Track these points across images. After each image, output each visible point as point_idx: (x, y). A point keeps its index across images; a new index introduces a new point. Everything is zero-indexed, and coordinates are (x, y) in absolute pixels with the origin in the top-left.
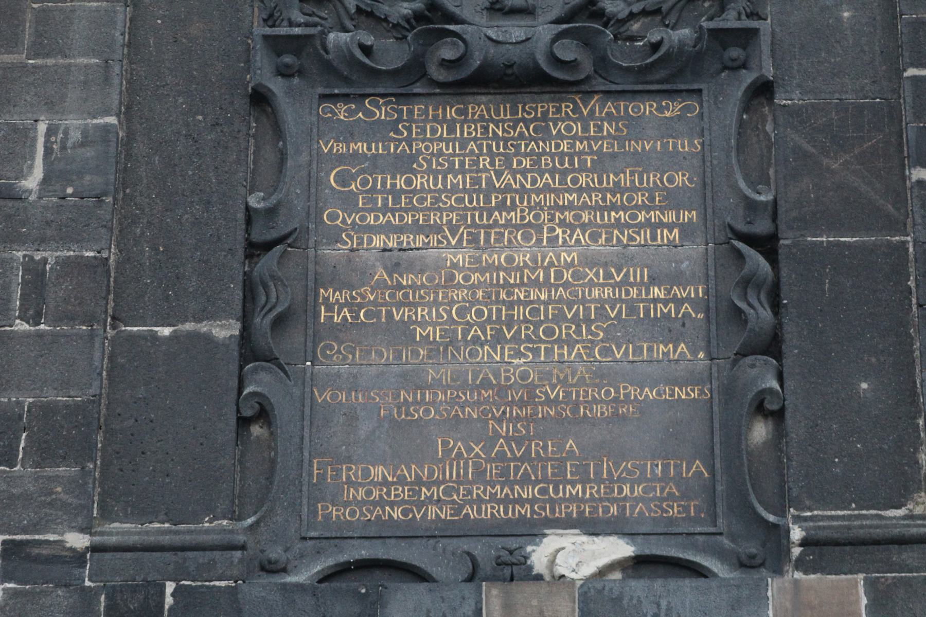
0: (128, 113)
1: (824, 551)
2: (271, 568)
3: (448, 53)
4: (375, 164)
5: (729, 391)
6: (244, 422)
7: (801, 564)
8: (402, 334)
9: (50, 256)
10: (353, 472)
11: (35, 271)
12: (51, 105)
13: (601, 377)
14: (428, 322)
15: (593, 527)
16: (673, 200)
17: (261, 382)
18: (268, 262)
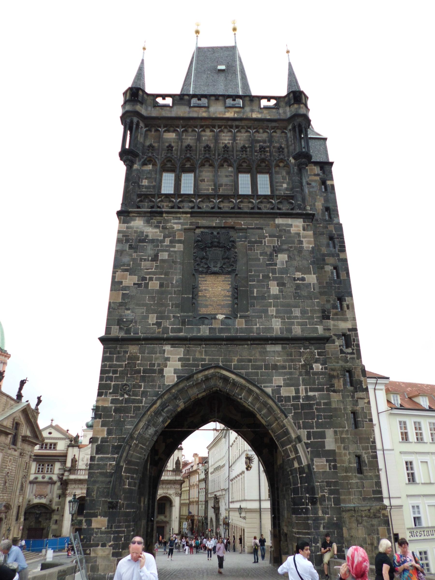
0: (182, 276)
1: (241, 317)
2: (195, 318)
3: (210, 271)
4: (204, 281)
5: (233, 302)
6: (192, 304)
7: (239, 318)
8: (206, 296)
9: (176, 289)
10: (201, 309)
11: (175, 290)
12: (176, 275)
13: (223, 300)
14: (208, 295)
15: (222, 314)
16: (229, 284)
17: (194, 301)
18: (194, 290)
